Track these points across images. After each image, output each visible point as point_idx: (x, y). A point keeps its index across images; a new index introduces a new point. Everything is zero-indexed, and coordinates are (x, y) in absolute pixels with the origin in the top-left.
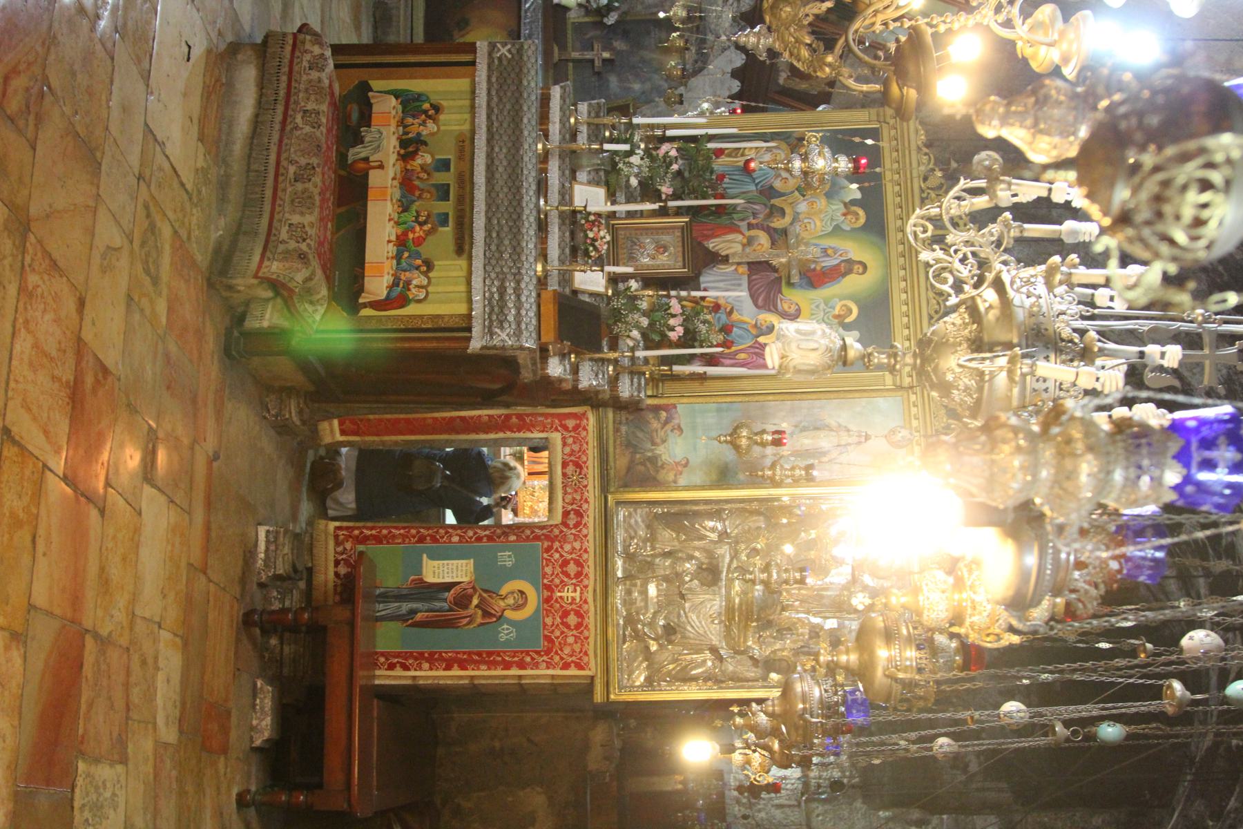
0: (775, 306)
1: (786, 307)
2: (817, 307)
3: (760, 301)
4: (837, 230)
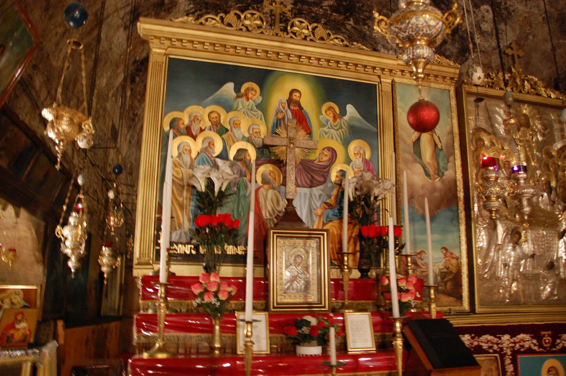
0: (325, 167)
1: (325, 159)
2: (326, 133)
3: (321, 179)
4: (262, 107)
